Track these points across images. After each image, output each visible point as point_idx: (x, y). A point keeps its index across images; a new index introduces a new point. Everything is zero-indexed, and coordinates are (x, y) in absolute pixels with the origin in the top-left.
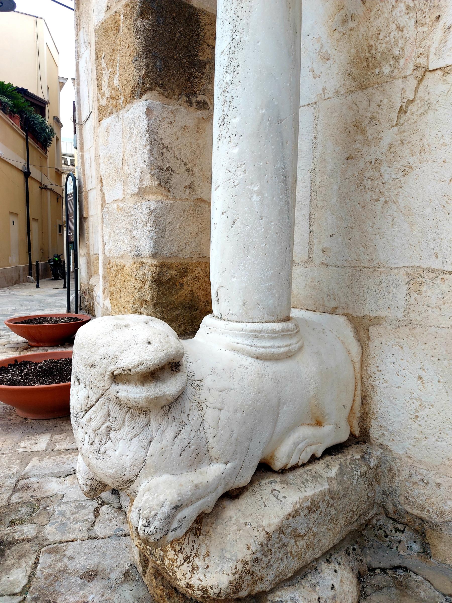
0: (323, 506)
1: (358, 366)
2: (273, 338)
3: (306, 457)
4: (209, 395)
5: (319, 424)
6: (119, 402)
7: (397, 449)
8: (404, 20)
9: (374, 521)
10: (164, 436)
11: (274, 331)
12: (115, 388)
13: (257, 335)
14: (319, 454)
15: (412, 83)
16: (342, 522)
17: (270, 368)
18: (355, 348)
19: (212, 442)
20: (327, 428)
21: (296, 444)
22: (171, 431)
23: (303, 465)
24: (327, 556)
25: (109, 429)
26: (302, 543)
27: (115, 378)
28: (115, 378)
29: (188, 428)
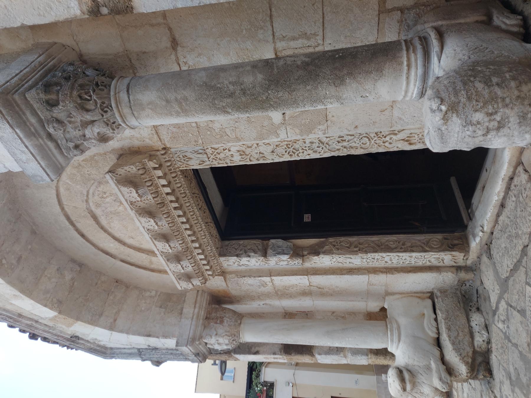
0: (450, 323)
1: (403, 295)
2: (393, 335)
3: (434, 323)
4: (411, 362)
5: (424, 314)
6: (412, 390)
7: (433, 286)
9: (463, 292)
10: (422, 378)
11: (391, 335)
12: (407, 391)
13: (392, 341)
14: (434, 316)
16: (458, 313)
17: (403, 338)
18: (397, 296)
19: (424, 364)
20: (426, 312)
21: (429, 329)
22: (421, 376)
23: (438, 324)
24: (469, 321)
25: (420, 392)
26: (461, 334)
27: (404, 389)
28: (404, 389)
29: (420, 371)
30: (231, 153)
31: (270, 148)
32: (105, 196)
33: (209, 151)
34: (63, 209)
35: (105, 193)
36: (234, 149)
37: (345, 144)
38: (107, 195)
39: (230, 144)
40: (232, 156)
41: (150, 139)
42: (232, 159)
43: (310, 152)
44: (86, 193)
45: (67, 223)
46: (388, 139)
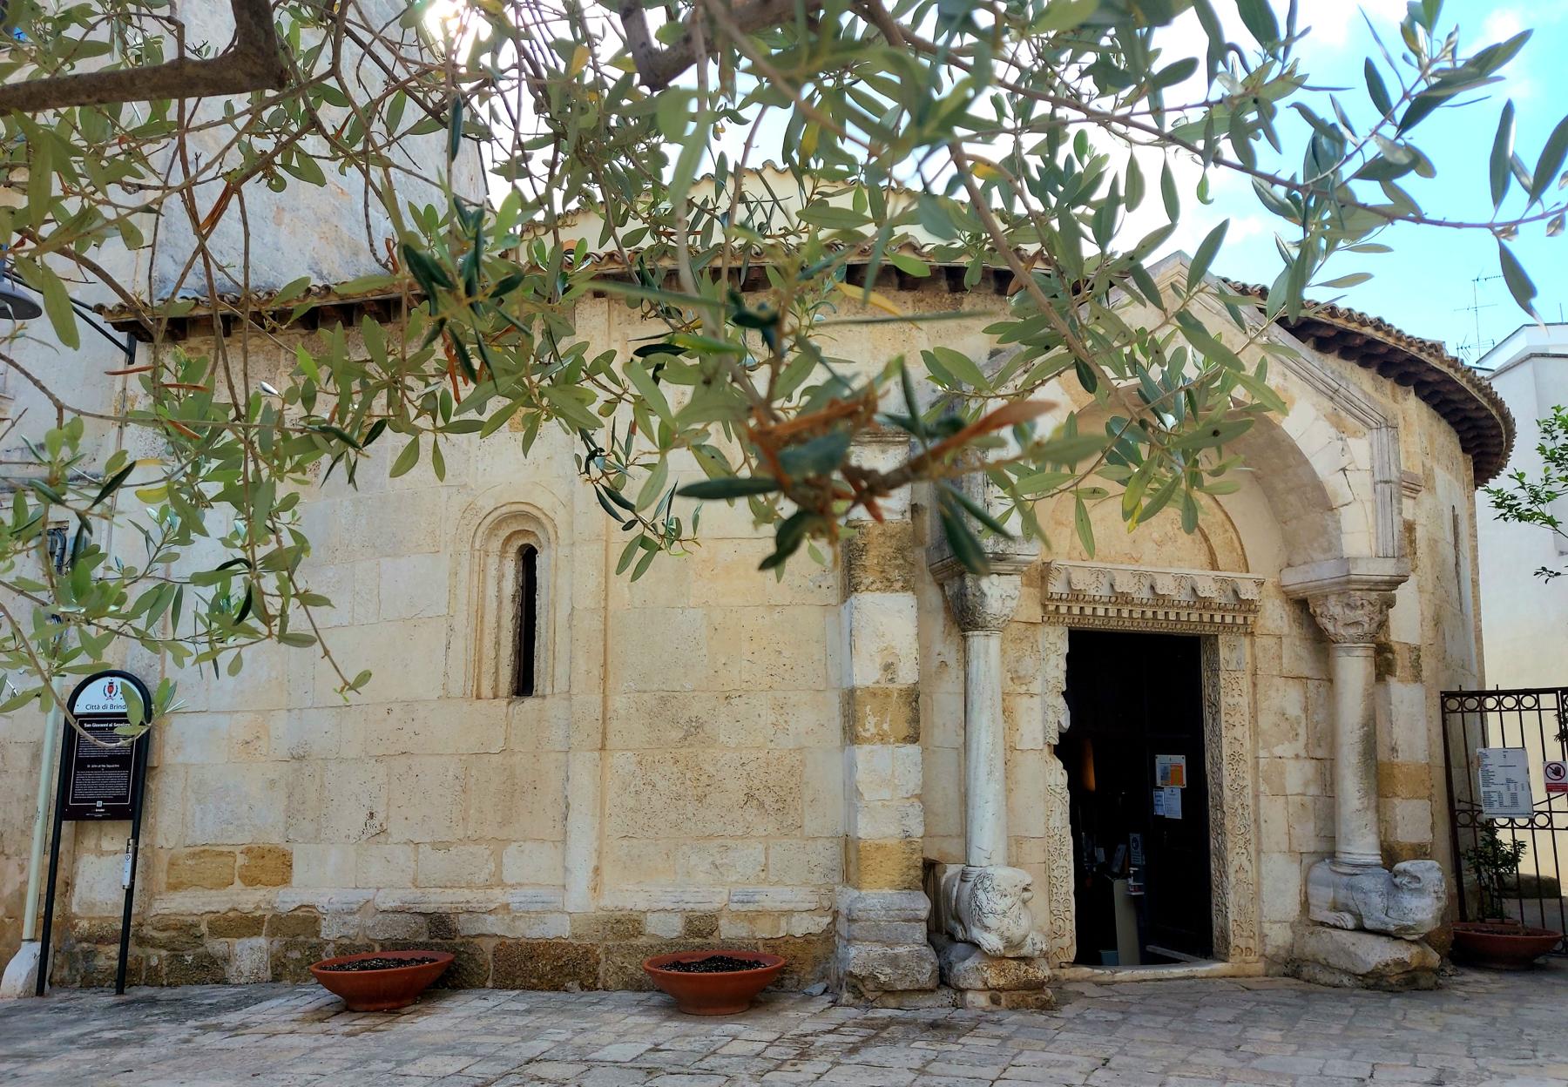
33: (1239, 675)
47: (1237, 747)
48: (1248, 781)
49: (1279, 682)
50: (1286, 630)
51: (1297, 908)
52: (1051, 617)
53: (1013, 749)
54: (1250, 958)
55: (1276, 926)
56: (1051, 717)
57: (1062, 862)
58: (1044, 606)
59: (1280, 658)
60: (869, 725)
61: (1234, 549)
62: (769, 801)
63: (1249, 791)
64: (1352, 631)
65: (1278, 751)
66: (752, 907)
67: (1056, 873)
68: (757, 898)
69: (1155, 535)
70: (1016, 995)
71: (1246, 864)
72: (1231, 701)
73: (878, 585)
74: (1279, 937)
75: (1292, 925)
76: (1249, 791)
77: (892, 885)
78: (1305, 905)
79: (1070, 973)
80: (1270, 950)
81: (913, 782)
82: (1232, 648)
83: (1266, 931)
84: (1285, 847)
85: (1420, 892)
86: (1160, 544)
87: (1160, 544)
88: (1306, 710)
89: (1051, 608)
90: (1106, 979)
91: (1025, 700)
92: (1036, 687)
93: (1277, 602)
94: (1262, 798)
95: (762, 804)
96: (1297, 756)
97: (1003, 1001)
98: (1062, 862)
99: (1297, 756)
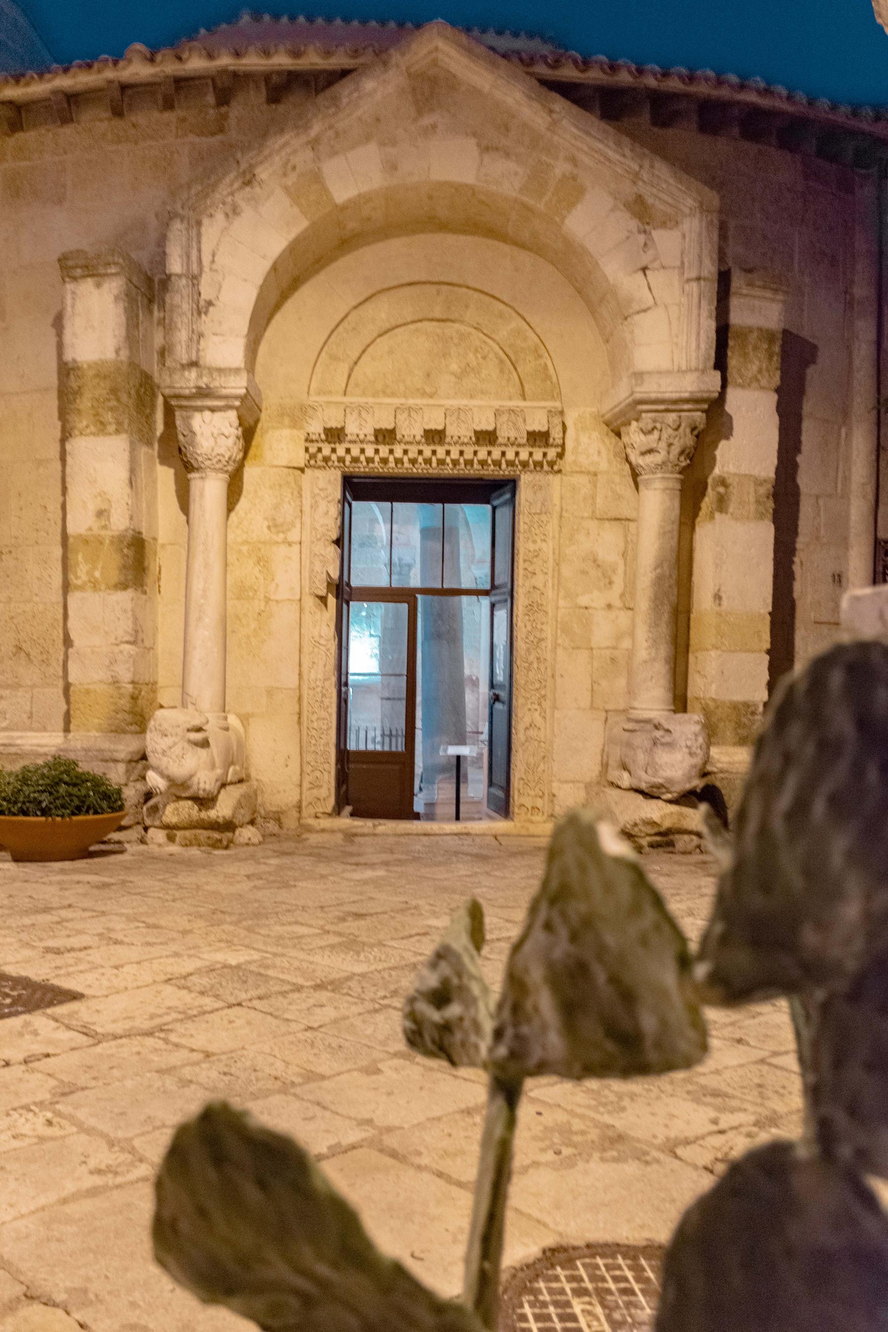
7: (264, 779)
8: (258, 575)
15: (263, 604)
30: (539, 541)
31: (540, 585)
32: (479, 356)
33: (544, 518)
34: (468, 287)
35: (484, 358)
36: (544, 546)
37: (535, 665)
38: (481, 360)
39: (551, 544)
40: (534, 542)
41: (575, 462)
42: (530, 542)
43: (529, 628)
44: (493, 336)
45: (442, 279)
46: (536, 707)
47: (536, 596)
48: (548, 632)
49: (593, 525)
50: (604, 466)
51: (597, 768)
52: (314, 461)
53: (267, 600)
54: (538, 818)
55: (567, 787)
56: (318, 567)
57: (323, 714)
58: (307, 450)
59: (593, 498)
60: (81, 572)
61: (548, 377)
62: (34, 653)
63: (549, 643)
64: (650, 459)
65: (583, 601)
66: (13, 750)
67: (315, 725)
68: (18, 742)
69: (454, 367)
70: (188, 833)
71: (538, 720)
72: (531, 547)
73: (93, 428)
74: (569, 797)
75: (588, 786)
76: (549, 643)
77: (99, 729)
78: (605, 766)
79: (326, 823)
80: (559, 811)
81: (124, 627)
82: (537, 488)
83: (555, 791)
84: (585, 702)
85: (670, 745)
86: (459, 377)
87: (459, 377)
88: (624, 555)
89: (313, 450)
90: (365, 831)
91: (283, 550)
92: (294, 535)
93: (595, 435)
94: (560, 651)
95: (28, 655)
96: (609, 606)
97: (177, 839)
98: (323, 714)
99: (609, 606)
